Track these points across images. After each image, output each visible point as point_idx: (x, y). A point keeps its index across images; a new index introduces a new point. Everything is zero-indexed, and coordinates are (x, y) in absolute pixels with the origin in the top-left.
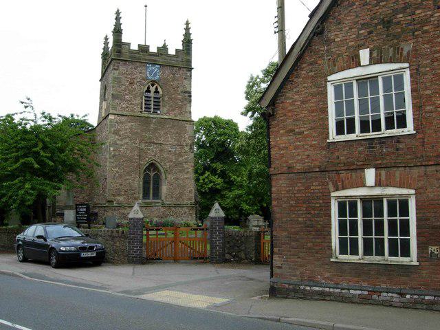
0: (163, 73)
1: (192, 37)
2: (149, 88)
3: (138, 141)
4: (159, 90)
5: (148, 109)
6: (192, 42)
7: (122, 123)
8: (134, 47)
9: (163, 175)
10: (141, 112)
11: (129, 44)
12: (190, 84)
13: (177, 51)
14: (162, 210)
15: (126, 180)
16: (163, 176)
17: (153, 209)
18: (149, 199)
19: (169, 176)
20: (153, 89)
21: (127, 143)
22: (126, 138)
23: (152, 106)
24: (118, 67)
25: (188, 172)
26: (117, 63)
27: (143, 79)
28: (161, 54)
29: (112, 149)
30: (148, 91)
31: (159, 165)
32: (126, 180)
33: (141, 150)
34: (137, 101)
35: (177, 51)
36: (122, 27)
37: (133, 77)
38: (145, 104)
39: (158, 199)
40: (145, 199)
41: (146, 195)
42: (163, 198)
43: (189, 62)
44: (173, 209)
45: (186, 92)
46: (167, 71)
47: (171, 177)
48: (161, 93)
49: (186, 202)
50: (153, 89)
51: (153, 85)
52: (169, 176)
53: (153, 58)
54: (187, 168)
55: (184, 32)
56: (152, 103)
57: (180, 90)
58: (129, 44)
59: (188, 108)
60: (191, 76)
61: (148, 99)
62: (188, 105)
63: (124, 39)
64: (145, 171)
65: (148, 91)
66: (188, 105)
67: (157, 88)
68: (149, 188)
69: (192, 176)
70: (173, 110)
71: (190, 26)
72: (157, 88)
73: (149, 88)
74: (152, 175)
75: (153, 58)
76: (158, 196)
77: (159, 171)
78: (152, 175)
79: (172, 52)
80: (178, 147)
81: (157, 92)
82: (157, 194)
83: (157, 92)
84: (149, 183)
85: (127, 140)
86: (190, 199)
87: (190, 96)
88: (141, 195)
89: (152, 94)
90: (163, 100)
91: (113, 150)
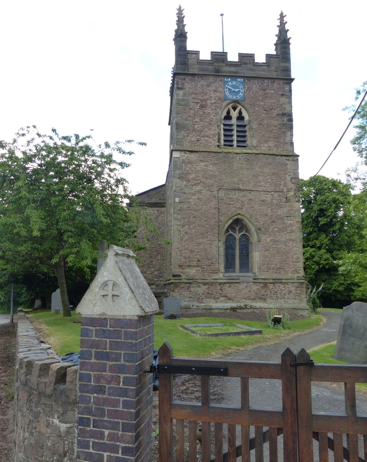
0: (249, 89)
1: (289, 35)
2: (228, 112)
3: (215, 189)
4: (245, 114)
5: (228, 143)
6: (291, 41)
7: (190, 162)
8: (205, 56)
9: (255, 235)
10: (218, 146)
11: (197, 53)
12: (290, 103)
13: (268, 56)
14: (255, 287)
15: (199, 244)
16: (254, 238)
17: (241, 286)
18: (234, 272)
19: (263, 238)
20: (234, 114)
21: (200, 191)
22: (198, 184)
23: (235, 138)
24: (183, 84)
25: (292, 232)
26: (181, 79)
27: (220, 99)
28: (245, 64)
29: (177, 200)
30: (228, 117)
31: (247, 222)
32: (199, 244)
33: (219, 200)
34: (213, 131)
35: (268, 56)
36: (186, 29)
37: (205, 97)
38: (225, 135)
39: (248, 271)
40: (229, 272)
41: (229, 266)
42: (256, 270)
43: (288, 70)
44: (271, 286)
45: (284, 115)
46: (255, 86)
47: (266, 239)
48: (247, 118)
49: (290, 275)
50: (234, 114)
51: (235, 108)
52: (263, 238)
53: (233, 69)
54: (291, 224)
55: (277, 31)
56: (235, 133)
57: (275, 112)
58: (197, 53)
59: (288, 138)
60: (290, 91)
61: (228, 130)
62: (289, 133)
63: (190, 46)
64: (227, 231)
65: (228, 117)
66: (289, 133)
67: (240, 113)
68: (234, 255)
69: (298, 235)
70: (266, 142)
71: (285, 19)
72: (240, 113)
73: (228, 112)
74: (238, 236)
75: (233, 69)
76: (248, 267)
77: (248, 230)
78: (238, 236)
79: (260, 59)
80: (276, 195)
81: (240, 118)
82: (245, 264)
83: (240, 118)
84: (233, 249)
85: (199, 188)
86: (297, 272)
87: (291, 120)
88: (222, 267)
89: (234, 121)
90: (251, 129)
91: (180, 202)
